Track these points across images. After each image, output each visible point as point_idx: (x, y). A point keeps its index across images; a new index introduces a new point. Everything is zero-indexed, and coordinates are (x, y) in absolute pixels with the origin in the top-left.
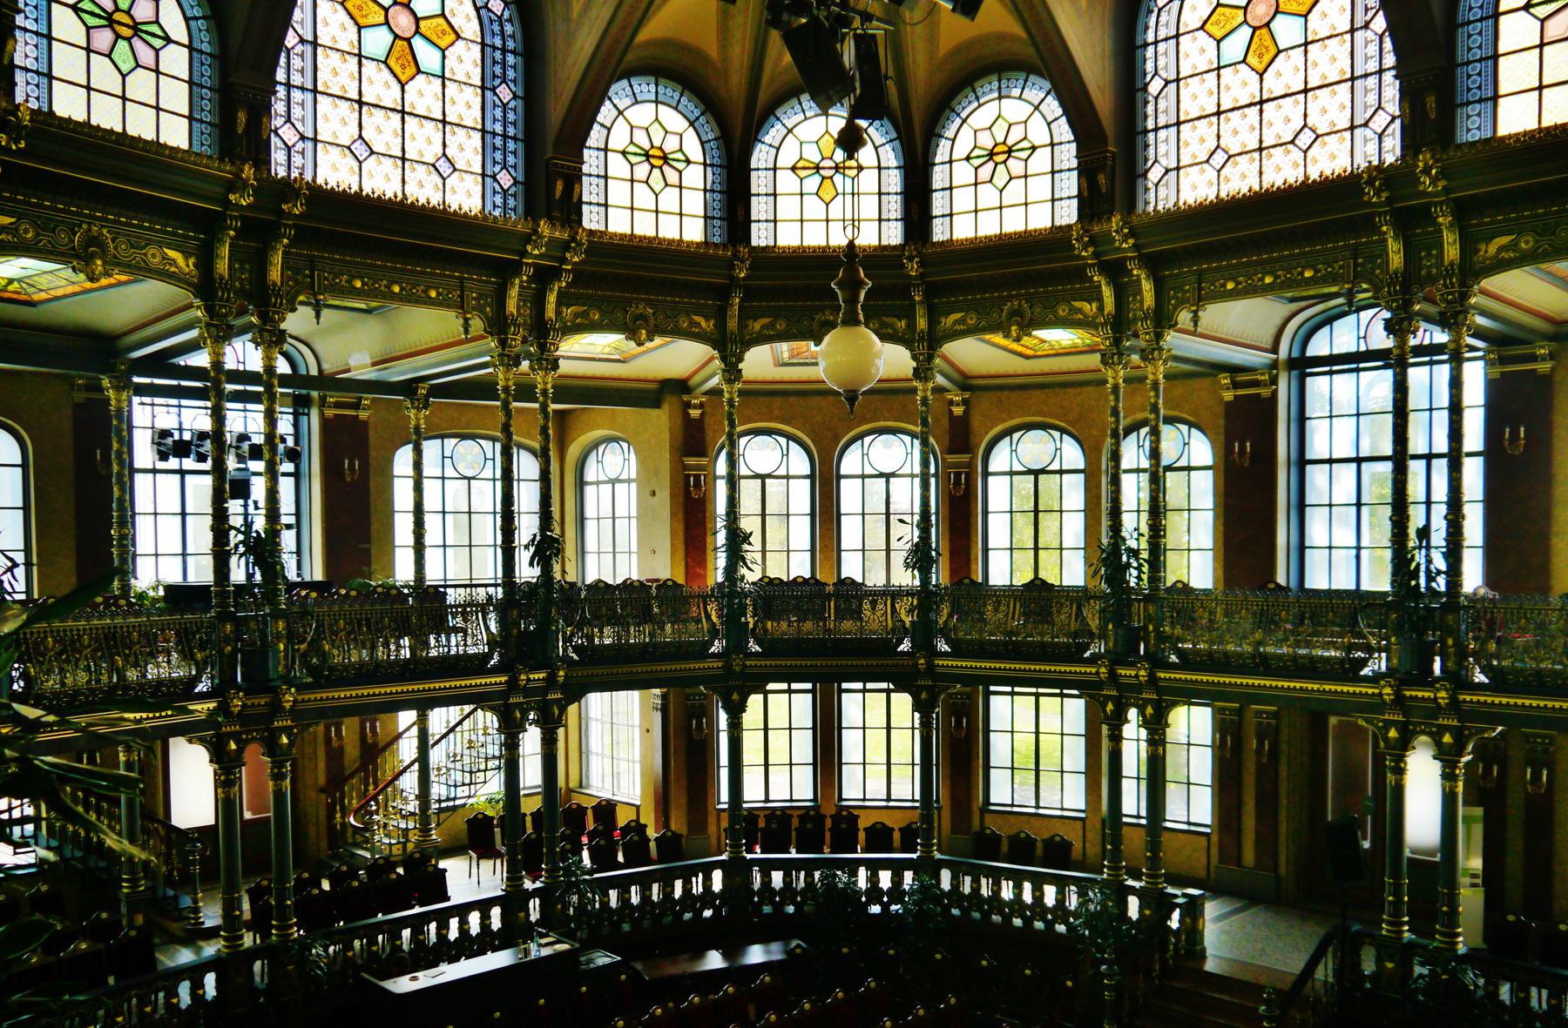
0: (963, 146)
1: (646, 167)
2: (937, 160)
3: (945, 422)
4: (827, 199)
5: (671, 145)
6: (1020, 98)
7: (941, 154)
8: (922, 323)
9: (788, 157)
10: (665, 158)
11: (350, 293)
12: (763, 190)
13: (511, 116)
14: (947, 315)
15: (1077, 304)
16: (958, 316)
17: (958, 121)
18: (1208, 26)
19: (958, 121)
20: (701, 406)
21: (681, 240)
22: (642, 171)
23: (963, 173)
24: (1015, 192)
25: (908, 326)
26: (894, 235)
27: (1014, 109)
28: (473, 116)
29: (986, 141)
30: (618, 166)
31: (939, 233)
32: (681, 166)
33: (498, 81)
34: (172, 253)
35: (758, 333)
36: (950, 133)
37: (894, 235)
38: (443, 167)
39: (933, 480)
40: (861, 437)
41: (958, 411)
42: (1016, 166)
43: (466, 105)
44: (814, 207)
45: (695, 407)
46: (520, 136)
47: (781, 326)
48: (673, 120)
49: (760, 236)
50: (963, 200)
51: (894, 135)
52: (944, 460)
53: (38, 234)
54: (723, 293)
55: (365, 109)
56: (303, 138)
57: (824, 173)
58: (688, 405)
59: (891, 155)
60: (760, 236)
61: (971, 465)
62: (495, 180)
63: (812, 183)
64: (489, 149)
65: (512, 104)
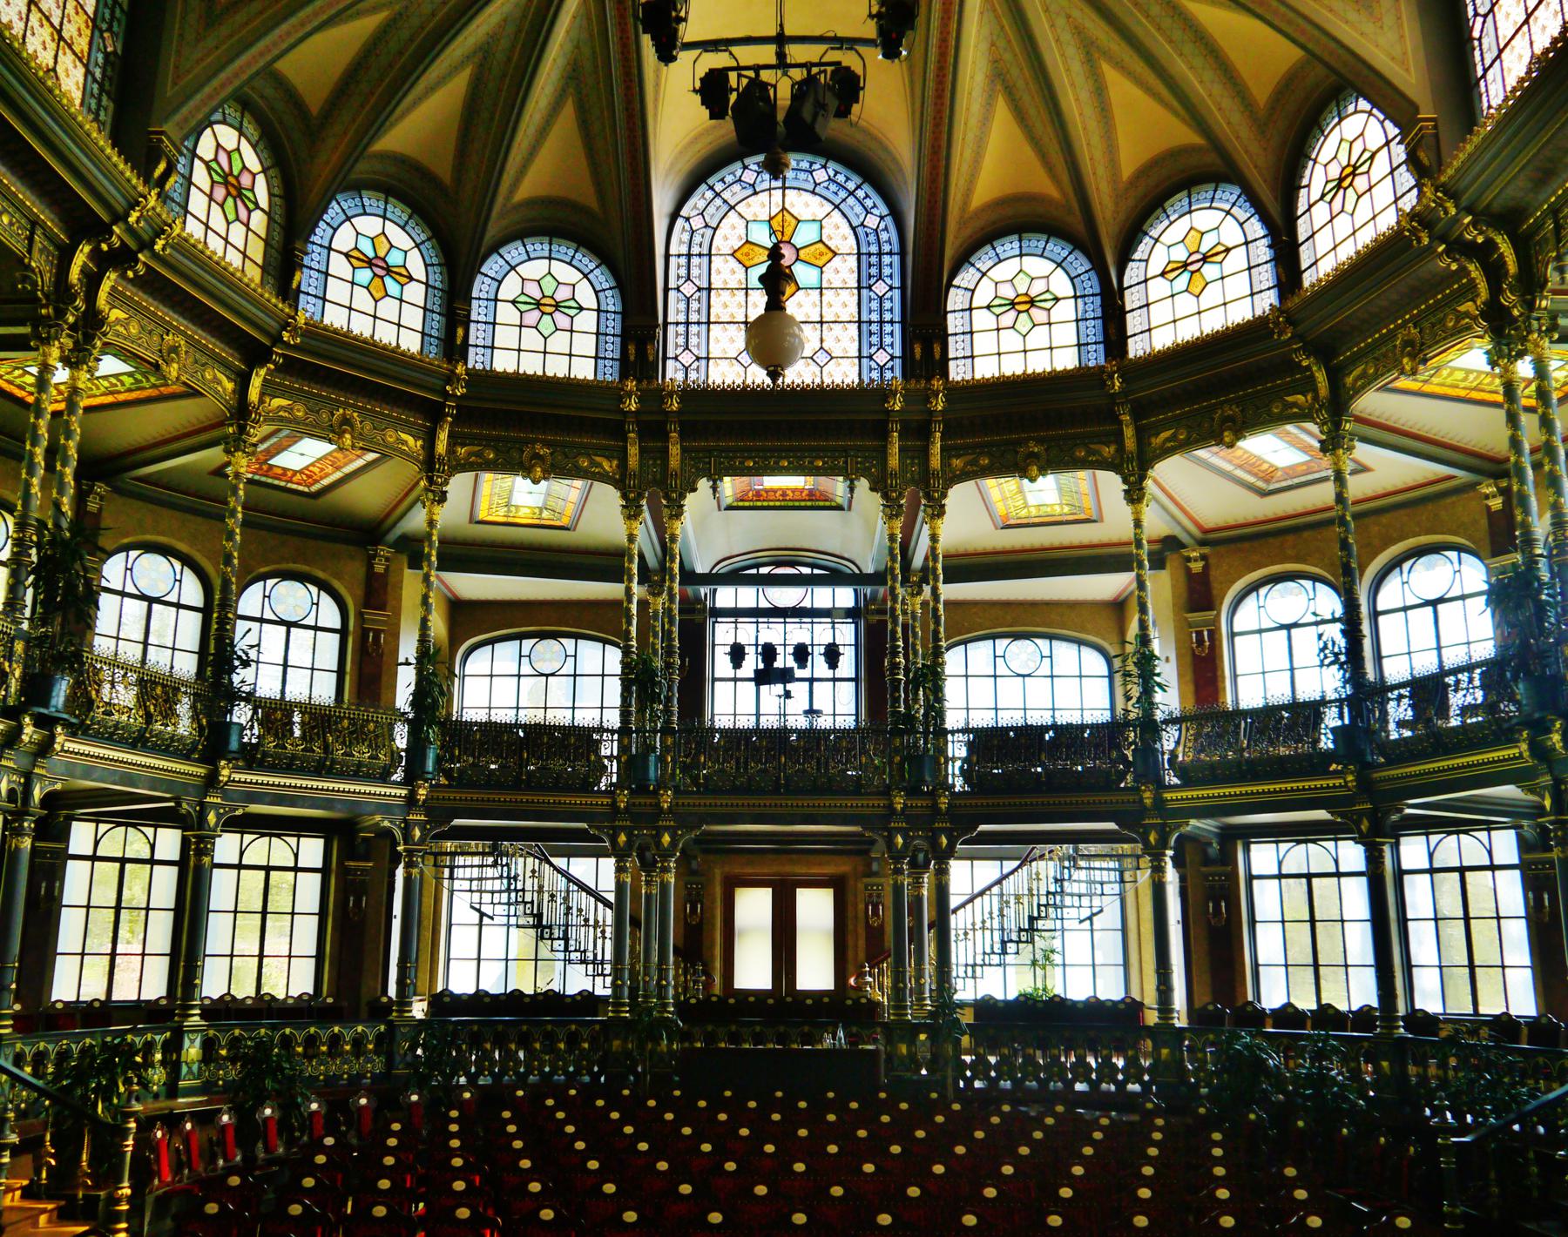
15: (598, 459)
18: (738, 255)
22: (220, 193)
24: (559, 342)
32: (251, 206)
42: (562, 321)
44: (363, 300)
63: (364, 275)
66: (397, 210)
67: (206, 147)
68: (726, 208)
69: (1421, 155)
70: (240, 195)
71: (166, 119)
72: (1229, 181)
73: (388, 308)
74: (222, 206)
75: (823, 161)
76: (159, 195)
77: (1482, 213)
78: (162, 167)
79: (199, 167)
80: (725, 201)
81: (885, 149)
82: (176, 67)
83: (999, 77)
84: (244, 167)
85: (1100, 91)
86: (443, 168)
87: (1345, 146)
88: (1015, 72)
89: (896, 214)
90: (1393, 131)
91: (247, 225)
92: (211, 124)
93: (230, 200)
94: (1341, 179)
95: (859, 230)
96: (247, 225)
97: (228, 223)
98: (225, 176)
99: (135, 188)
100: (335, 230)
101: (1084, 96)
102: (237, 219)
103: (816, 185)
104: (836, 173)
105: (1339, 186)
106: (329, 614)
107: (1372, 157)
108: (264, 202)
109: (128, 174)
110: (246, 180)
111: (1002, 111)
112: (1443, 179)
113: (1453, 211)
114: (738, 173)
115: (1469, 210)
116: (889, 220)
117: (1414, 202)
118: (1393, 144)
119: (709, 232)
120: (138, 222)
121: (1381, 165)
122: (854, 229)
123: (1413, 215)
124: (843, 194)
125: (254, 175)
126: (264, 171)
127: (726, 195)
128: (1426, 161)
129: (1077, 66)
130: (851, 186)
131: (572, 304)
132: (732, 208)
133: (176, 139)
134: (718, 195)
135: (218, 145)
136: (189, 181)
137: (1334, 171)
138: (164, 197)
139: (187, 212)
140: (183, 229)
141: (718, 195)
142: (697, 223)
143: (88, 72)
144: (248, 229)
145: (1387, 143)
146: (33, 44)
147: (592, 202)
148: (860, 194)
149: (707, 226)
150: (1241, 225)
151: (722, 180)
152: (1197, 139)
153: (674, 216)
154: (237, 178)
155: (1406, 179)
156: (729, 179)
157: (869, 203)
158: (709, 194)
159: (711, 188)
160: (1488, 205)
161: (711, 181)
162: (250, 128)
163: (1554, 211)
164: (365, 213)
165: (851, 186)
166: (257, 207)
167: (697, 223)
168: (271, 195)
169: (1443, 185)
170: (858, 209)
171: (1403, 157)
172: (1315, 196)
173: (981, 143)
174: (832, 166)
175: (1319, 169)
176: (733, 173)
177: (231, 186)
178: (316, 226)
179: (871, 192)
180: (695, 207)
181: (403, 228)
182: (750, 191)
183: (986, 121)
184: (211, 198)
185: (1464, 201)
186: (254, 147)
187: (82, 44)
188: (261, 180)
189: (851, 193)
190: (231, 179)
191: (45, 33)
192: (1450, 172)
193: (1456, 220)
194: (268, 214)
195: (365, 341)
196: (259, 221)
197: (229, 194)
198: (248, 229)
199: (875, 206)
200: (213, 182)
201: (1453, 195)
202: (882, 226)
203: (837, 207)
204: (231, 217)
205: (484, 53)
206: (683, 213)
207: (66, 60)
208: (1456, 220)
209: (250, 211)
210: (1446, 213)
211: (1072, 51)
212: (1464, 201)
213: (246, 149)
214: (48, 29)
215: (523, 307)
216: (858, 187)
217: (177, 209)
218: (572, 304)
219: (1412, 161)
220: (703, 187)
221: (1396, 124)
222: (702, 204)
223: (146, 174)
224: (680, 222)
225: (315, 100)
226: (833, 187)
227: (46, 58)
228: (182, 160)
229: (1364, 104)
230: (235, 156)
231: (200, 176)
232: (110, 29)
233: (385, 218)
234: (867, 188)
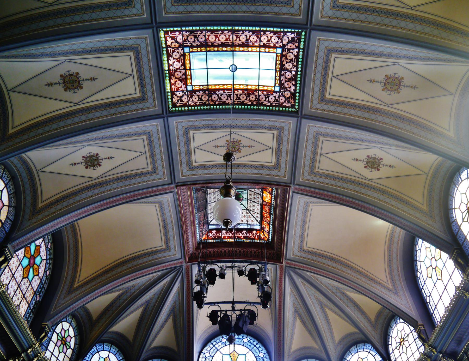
22: (59, 343)
32: (68, 347)
66: (114, 349)
67: (58, 329)
68: (216, 350)
69: (422, 336)
70: (65, 344)
71: (48, 320)
72: (368, 343)
74: (59, 347)
75: (246, 336)
76: (40, 344)
77: (444, 354)
78: (43, 335)
79: (55, 335)
80: (216, 348)
81: (265, 332)
82: (56, 305)
83: (296, 312)
84: (69, 335)
85: (326, 316)
86: (130, 337)
87: (399, 332)
88: (301, 311)
89: (269, 352)
90: (412, 328)
91: (65, 354)
92: (62, 322)
93: (62, 345)
94: (401, 342)
95: (258, 358)
96: (65, 354)
97: (60, 353)
98: (62, 338)
99: (33, 342)
100: (93, 356)
101: (322, 318)
102: (63, 352)
103: (244, 343)
104: (250, 339)
105: (400, 344)
107: (408, 336)
108: (72, 346)
109: (32, 337)
110: (68, 339)
111: (298, 321)
112: (430, 343)
113: (436, 353)
114: (221, 339)
115: (440, 352)
116: (267, 354)
117: (424, 350)
118: (413, 332)
119: (211, 358)
120: (30, 352)
121: (411, 339)
122: (256, 357)
123: (424, 354)
124: (252, 346)
125: (71, 338)
126: (75, 336)
127: (217, 346)
128: (424, 337)
129: (318, 309)
130: (255, 343)
132: (218, 350)
133: (50, 326)
134: (214, 346)
135: (63, 328)
136: (50, 339)
137: (398, 341)
138: (41, 345)
139: (47, 349)
140: (44, 355)
141: (214, 346)
142: (207, 355)
143: (29, 306)
144: (65, 355)
145: (411, 332)
146: (15, 298)
147: (174, 347)
148: (258, 346)
149: (210, 356)
150: (374, 356)
151: (216, 341)
152: (356, 330)
153: (200, 352)
154: (66, 339)
155: (419, 343)
156: (218, 341)
157: (260, 349)
158: (211, 346)
159: (212, 344)
160: (446, 351)
161: (212, 342)
162: (74, 323)
163: (465, 353)
164: (104, 350)
165: (255, 343)
166: (70, 347)
167: (207, 355)
168: (75, 344)
169: (431, 345)
170: (257, 351)
171: (417, 336)
172: (394, 348)
173: (293, 331)
174: (249, 337)
175: (393, 339)
176: (219, 339)
177: (64, 341)
178: (87, 354)
179: (261, 346)
180: (207, 350)
181: (115, 355)
182: (224, 345)
183: (294, 324)
184: (56, 345)
185: (438, 349)
186: (73, 329)
187: (29, 299)
188: (73, 339)
189: (255, 346)
190: (64, 339)
191: (19, 295)
192: (432, 341)
193: (437, 356)
196: (69, 352)
197: (62, 343)
198: (65, 355)
199: (262, 350)
200: (58, 340)
201: (435, 348)
202: (265, 356)
203: (250, 350)
204: (61, 351)
205: (148, 303)
206: (203, 351)
207: (24, 303)
208: (437, 356)
209: (67, 349)
210: (434, 353)
211: (316, 305)
212: (438, 349)
213: (71, 330)
214: (21, 294)
216: (257, 344)
217: (44, 348)
219: (420, 337)
220: (210, 343)
221: (412, 326)
222: (209, 349)
223: (37, 337)
224: (202, 355)
225: (94, 317)
226: (249, 344)
227: (17, 303)
228: (50, 333)
229: (401, 320)
230: (67, 332)
231: (55, 338)
232: (39, 294)
233: (110, 352)
234: (260, 344)
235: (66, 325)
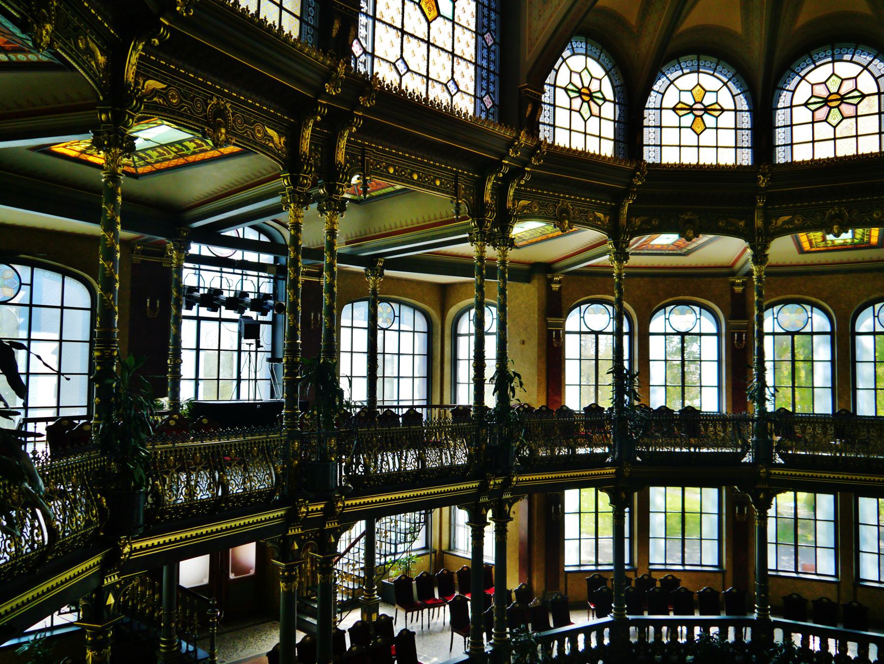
0: (803, 93)
1: (579, 100)
2: (779, 106)
3: (728, 297)
4: (699, 131)
5: (594, 86)
6: (851, 61)
7: (784, 100)
8: (759, 223)
9: (671, 99)
10: (590, 95)
11: (387, 177)
12: (652, 123)
13: (492, 57)
14: (778, 217)
16: (786, 218)
17: (797, 78)
19: (797, 78)
20: (559, 282)
21: (600, 155)
22: (576, 103)
23: (802, 115)
24: (847, 128)
25: (746, 225)
26: (746, 158)
27: (845, 69)
28: (469, 53)
29: (821, 91)
30: (562, 98)
31: (781, 156)
32: (600, 102)
33: (485, 30)
34: (270, 132)
35: (639, 227)
36: (791, 87)
37: (746, 158)
38: (452, 85)
39: (626, 339)
40: (664, 307)
41: (738, 289)
42: (848, 110)
43: (466, 44)
44: (689, 137)
45: (556, 282)
46: (497, 72)
47: (655, 222)
48: (597, 70)
49: (650, 156)
50: (802, 134)
51: (747, 88)
52: (727, 324)
53: (181, 101)
54: (618, 197)
55: (405, 37)
56: (365, 52)
57: (696, 113)
58: (551, 281)
59: (744, 102)
60: (650, 156)
61: (749, 329)
62: (482, 102)
63: (688, 120)
64: (479, 79)
65: (493, 48)
73: (708, 137)
79: (560, 93)
82: (530, 39)
106: (708, 324)
131: (856, 93)
186: (598, 61)
194: (614, 102)
195: (694, 166)
204: (586, 116)
215: (813, 107)
218: (856, 93)
235: (577, 62)
